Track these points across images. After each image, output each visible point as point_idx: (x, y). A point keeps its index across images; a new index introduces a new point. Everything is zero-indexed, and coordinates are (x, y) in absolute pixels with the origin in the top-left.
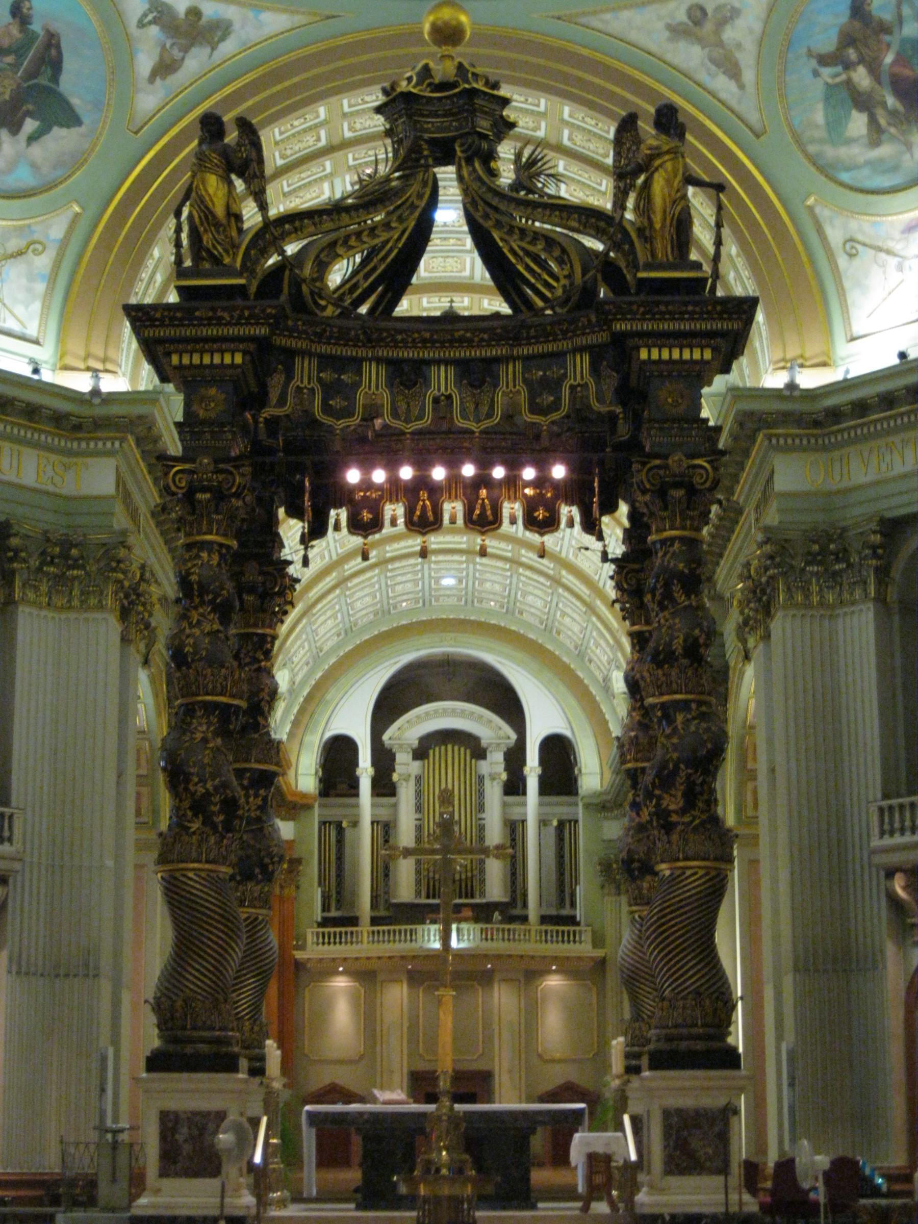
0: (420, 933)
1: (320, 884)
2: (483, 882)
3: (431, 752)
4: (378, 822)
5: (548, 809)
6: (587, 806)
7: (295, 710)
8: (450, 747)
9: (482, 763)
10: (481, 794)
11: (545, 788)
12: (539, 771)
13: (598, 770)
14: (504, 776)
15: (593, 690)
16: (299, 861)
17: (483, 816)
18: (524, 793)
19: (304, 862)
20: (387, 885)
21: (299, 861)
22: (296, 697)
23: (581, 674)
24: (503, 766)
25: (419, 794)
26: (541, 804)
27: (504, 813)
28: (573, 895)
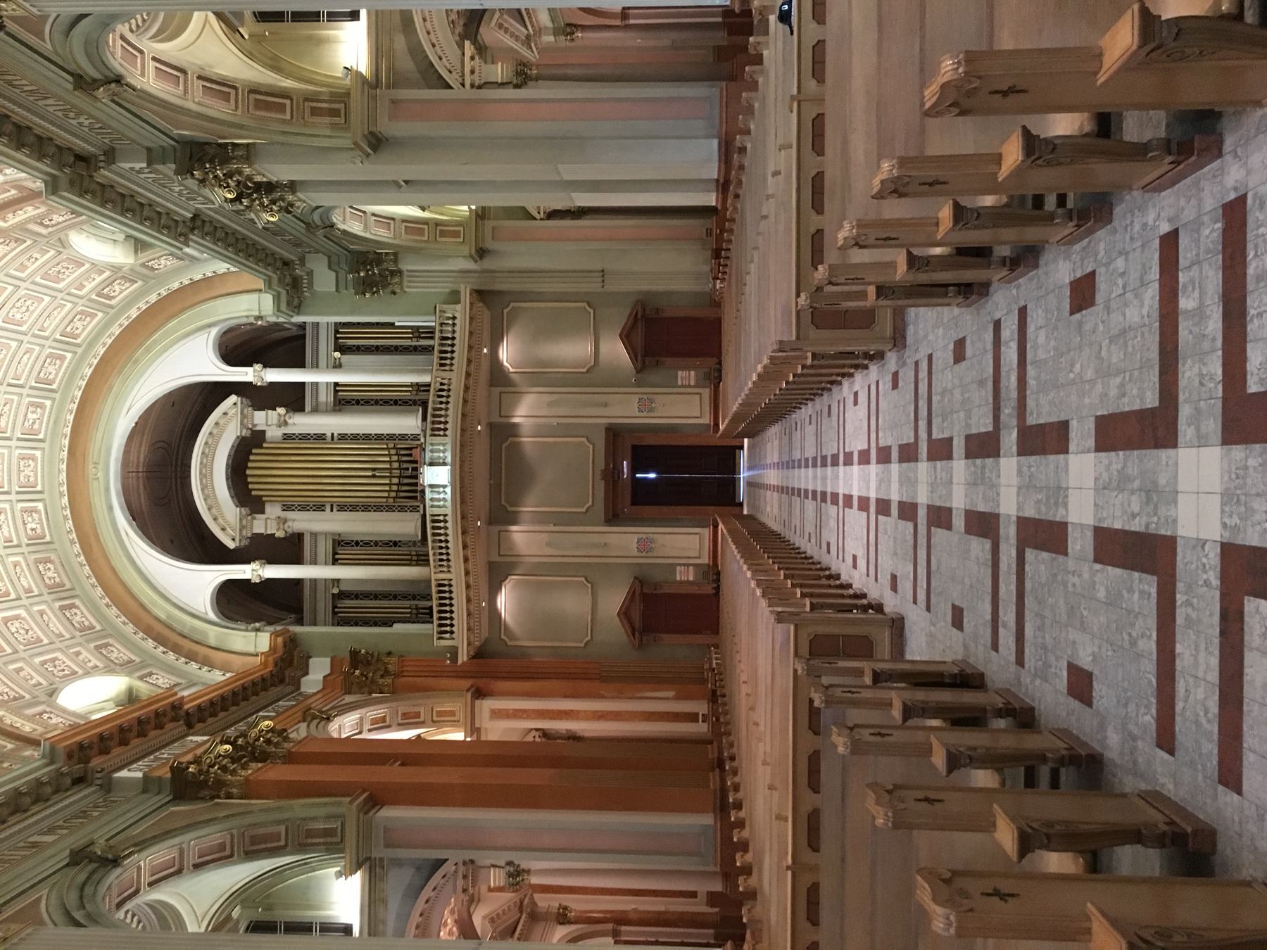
0: (436, 511)
1: (391, 626)
2: (403, 437)
3: (254, 493)
4: (335, 553)
5: (322, 361)
6: (298, 308)
7: (171, 656)
8: (248, 472)
9: (269, 435)
10: (305, 437)
11: (300, 363)
12: (258, 367)
13: (255, 296)
14: (281, 410)
15: (153, 298)
16: (354, 654)
17: (329, 435)
18: (303, 384)
19: (357, 647)
20: (406, 544)
21: (354, 654)
22: (153, 657)
23: (134, 313)
24: (270, 412)
25: (304, 508)
26: (316, 366)
27: (326, 412)
28: (417, 332)
